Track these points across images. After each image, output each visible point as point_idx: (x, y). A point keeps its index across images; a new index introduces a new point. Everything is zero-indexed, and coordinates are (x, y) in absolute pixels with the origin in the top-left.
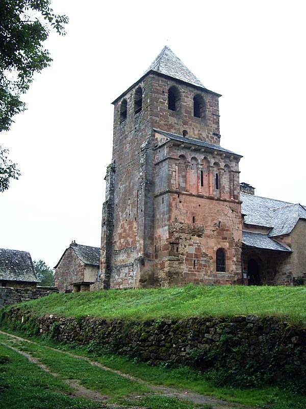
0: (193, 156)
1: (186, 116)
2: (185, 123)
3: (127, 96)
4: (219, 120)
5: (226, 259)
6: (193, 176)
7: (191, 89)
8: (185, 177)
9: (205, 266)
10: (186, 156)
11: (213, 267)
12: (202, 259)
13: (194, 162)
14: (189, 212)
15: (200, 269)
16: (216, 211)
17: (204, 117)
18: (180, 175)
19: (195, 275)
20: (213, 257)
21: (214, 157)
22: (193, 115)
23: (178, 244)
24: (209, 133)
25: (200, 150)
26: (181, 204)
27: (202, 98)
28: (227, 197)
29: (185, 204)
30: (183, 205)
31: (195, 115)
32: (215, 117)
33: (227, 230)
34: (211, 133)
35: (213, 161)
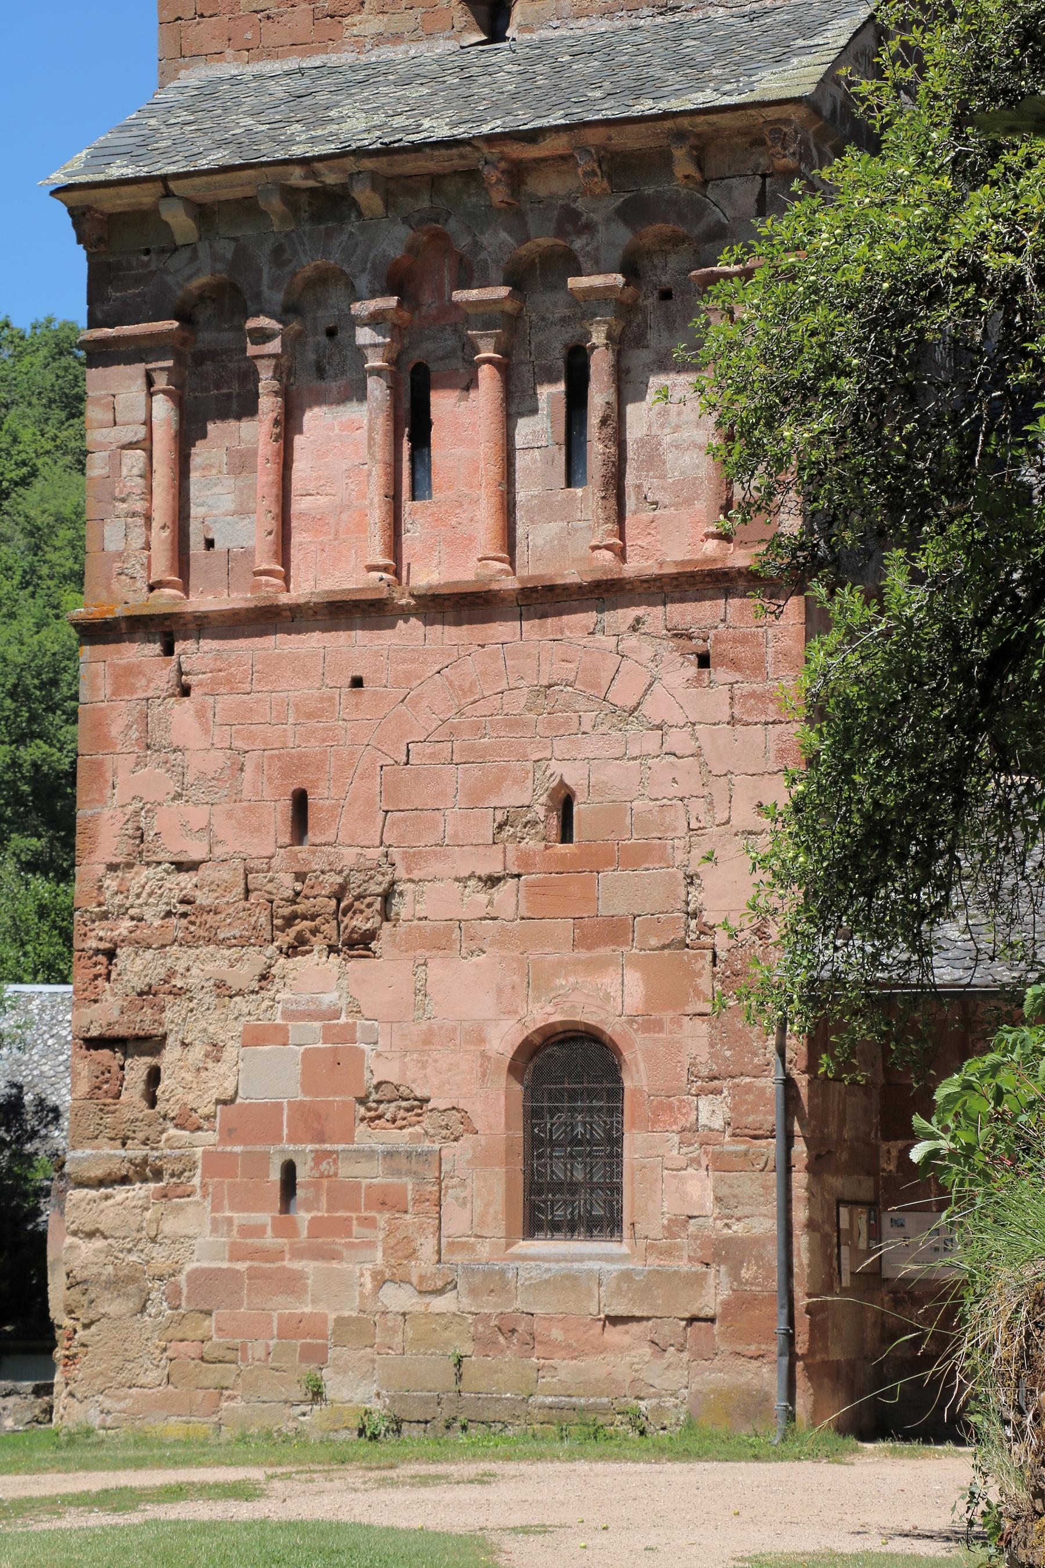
9: (388, 1201)
12: (366, 1137)
14: (250, 762)
15: (344, 1227)
19: (292, 1284)
20: (475, 1109)
23: (149, 1044)
29: (226, 701)
30: (200, 714)
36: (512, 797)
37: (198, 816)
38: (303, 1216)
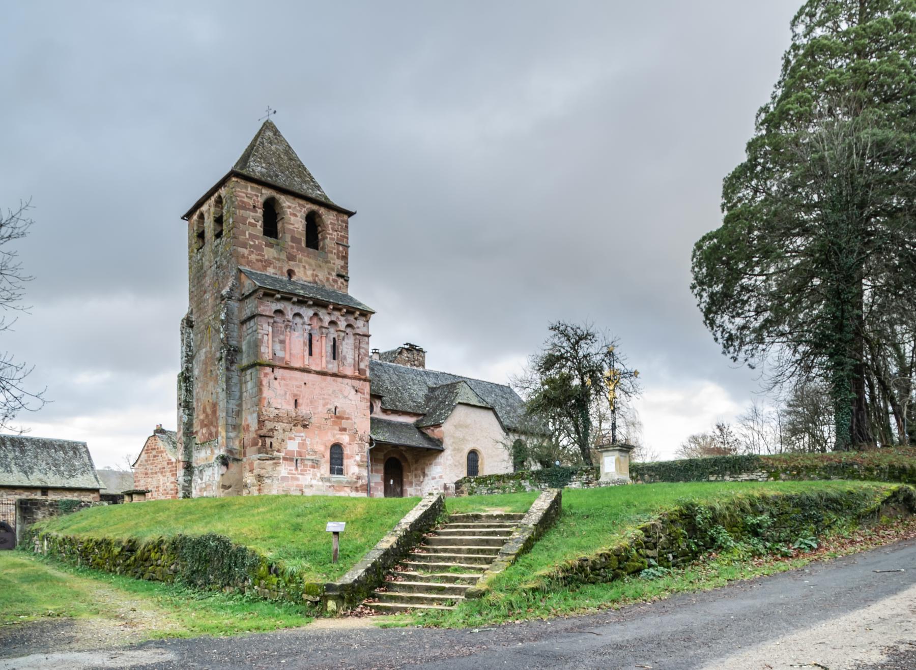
0: (296, 311)
1: (292, 247)
2: (291, 258)
3: (204, 208)
4: (347, 253)
5: (345, 457)
6: (297, 340)
7: (302, 202)
8: (282, 342)
10: (285, 312)
11: (325, 468)
13: (298, 320)
16: (330, 392)
17: (323, 248)
18: (277, 340)
19: (297, 479)
21: (329, 314)
22: (303, 244)
24: (329, 274)
25: (306, 302)
26: (276, 382)
27: (320, 216)
28: (349, 371)
29: (283, 382)
31: (308, 245)
32: (341, 248)
33: (348, 419)
34: (334, 274)
35: (327, 319)
36: (329, 406)
37: (279, 401)
38: (299, 469)
